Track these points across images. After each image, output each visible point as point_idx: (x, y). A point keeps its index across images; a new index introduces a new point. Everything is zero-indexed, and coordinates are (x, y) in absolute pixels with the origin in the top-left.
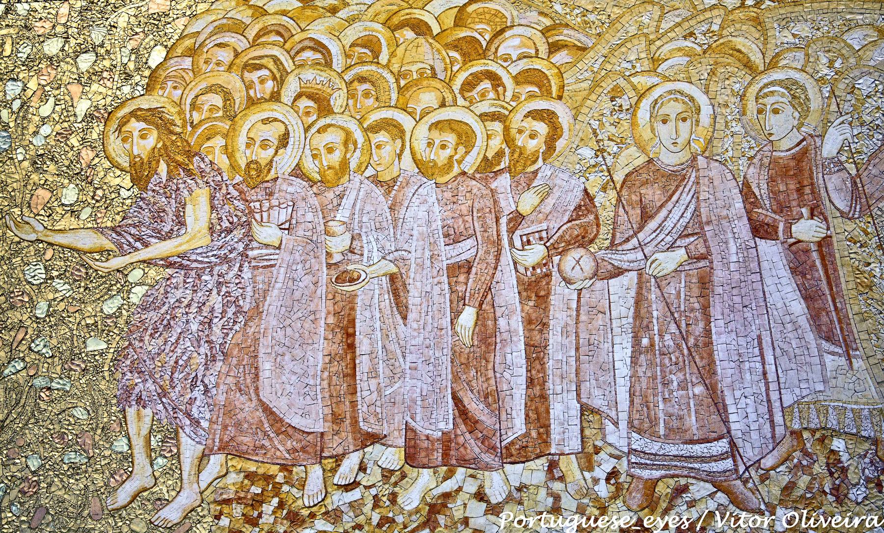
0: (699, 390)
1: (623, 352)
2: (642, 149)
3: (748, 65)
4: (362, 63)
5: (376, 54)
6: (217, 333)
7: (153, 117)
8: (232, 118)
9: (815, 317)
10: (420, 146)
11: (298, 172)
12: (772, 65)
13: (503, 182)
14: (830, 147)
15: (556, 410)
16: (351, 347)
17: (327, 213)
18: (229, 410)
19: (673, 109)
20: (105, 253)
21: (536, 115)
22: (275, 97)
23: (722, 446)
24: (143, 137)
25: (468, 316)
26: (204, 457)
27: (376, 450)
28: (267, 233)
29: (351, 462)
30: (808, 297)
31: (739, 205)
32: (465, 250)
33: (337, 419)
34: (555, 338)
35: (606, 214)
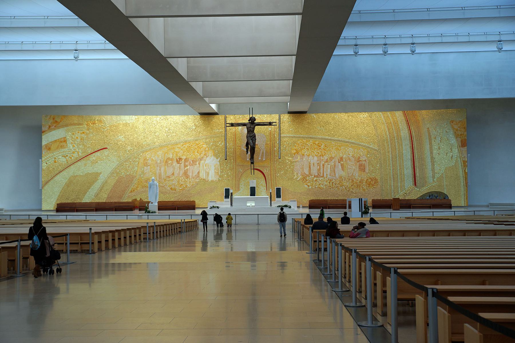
0: (334, 173)
1: (329, 170)
2: (331, 155)
3: (339, 150)
4: (311, 146)
5: (312, 146)
6: (301, 167)
7: (295, 149)
8: (301, 150)
9: (342, 169)
10: (315, 153)
11: (306, 155)
12: (341, 150)
13: (321, 157)
14: (344, 157)
15: (324, 174)
16: (310, 169)
17: (309, 158)
18: (302, 173)
19: (334, 153)
20: (292, 160)
21: (324, 152)
22: (304, 149)
23: (335, 177)
24: (295, 151)
25: (319, 167)
26: (300, 176)
27: (312, 176)
28: (304, 159)
29: (310, 177)
30: (342, 167)
31: (338, 160)
32: (319, 162)
33: (309, 174)
34: (325, 169)
35: (329, 160)
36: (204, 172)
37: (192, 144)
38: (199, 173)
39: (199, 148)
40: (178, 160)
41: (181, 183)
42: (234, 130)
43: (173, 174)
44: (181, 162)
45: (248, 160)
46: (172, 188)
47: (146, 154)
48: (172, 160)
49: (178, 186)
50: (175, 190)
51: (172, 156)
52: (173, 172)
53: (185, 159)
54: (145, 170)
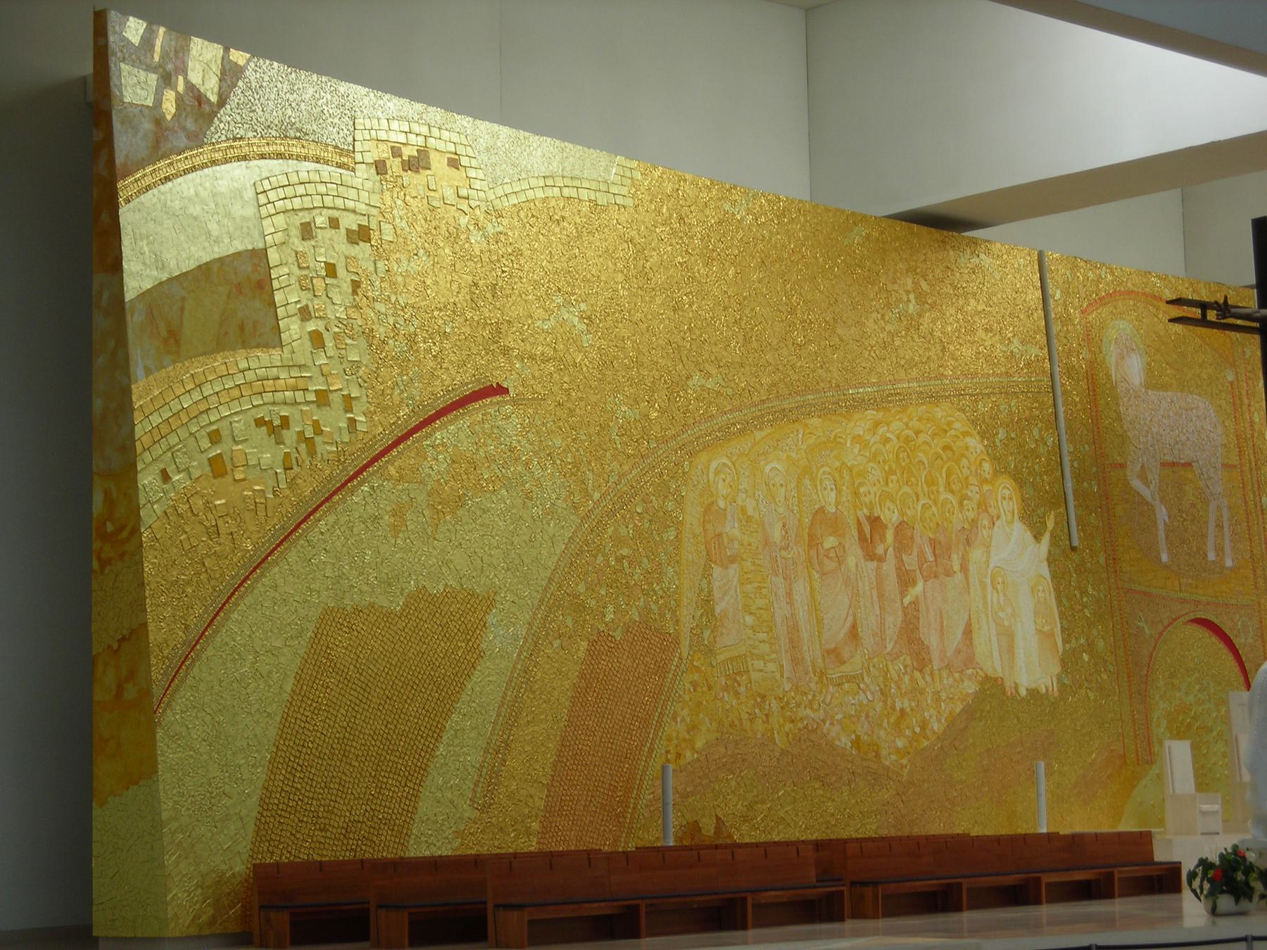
36: (993, 625)
37: (915, 423)
38: (968, 632)
39: (950, 454)
40: (867, 529)
41: (898, 706)
42: (1085, 353)
43: (854, 634)
44: (880, 550)
45: (1164, 557)
46: (858, 737)
47: (709, 462)
48: (835, 524)
49: (885, 724)
50: (877, 756)
51: (833, 494)
52: (850, 619)
53: (900, 528)
54: (717, 594)
